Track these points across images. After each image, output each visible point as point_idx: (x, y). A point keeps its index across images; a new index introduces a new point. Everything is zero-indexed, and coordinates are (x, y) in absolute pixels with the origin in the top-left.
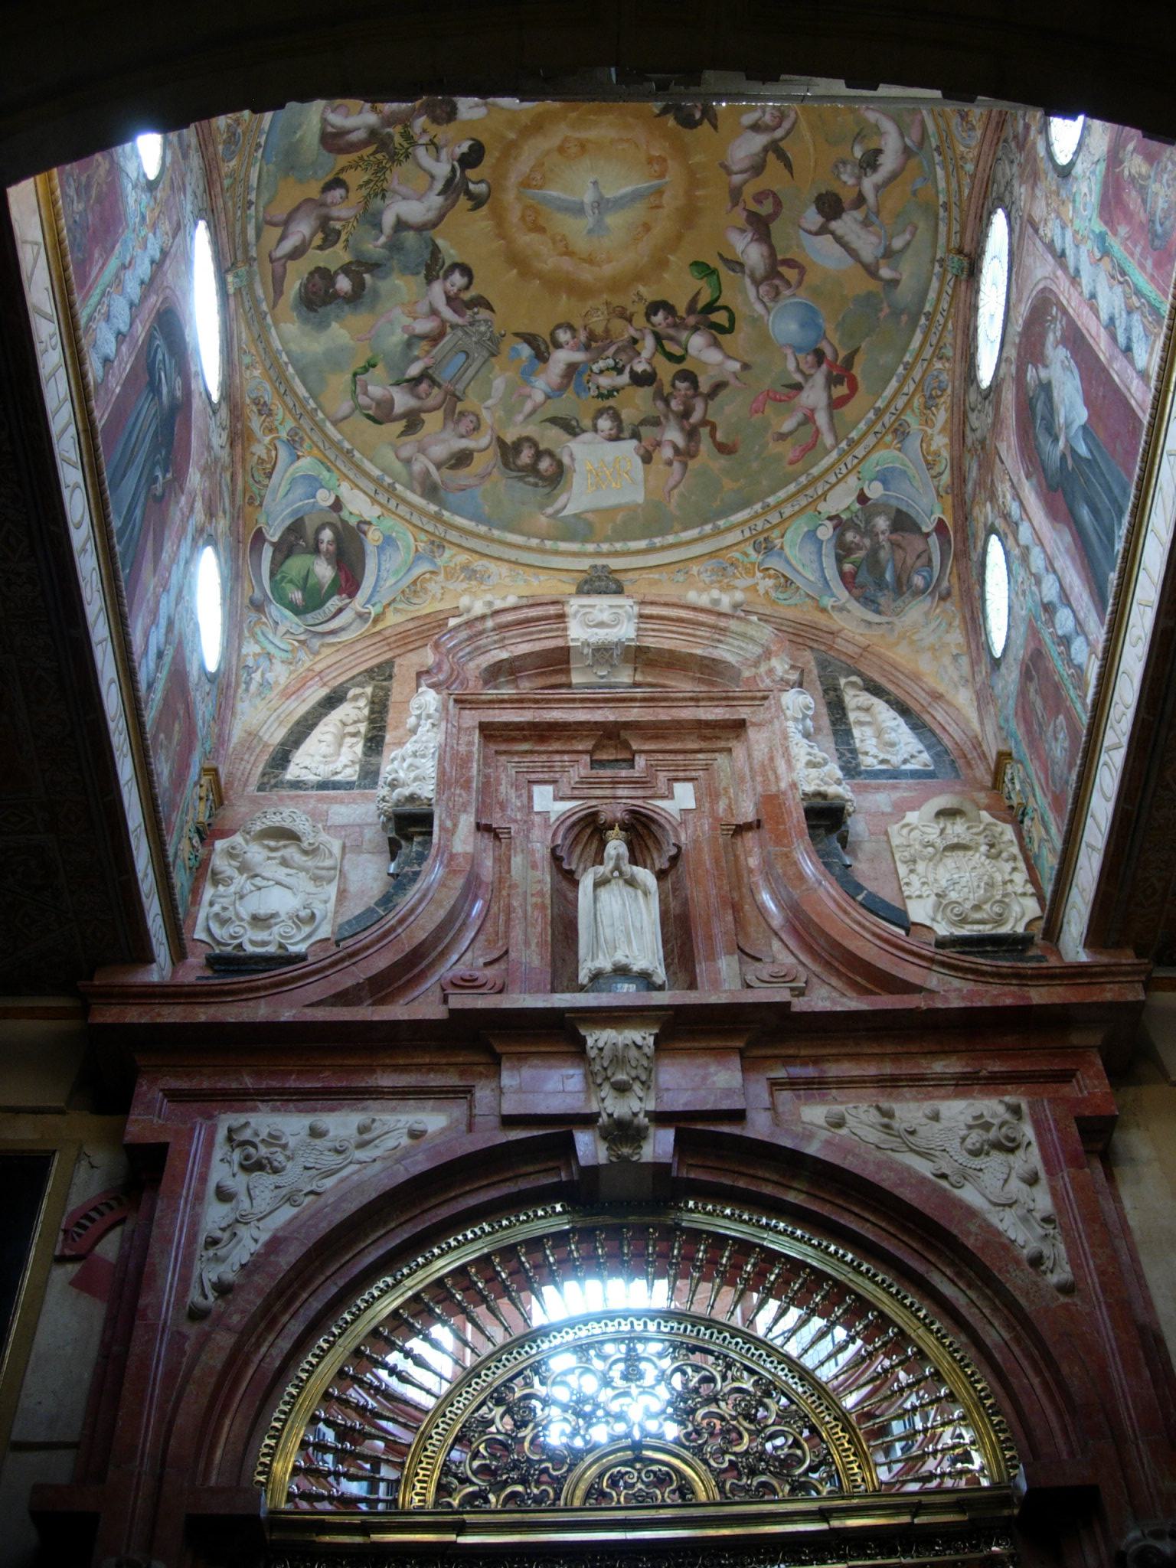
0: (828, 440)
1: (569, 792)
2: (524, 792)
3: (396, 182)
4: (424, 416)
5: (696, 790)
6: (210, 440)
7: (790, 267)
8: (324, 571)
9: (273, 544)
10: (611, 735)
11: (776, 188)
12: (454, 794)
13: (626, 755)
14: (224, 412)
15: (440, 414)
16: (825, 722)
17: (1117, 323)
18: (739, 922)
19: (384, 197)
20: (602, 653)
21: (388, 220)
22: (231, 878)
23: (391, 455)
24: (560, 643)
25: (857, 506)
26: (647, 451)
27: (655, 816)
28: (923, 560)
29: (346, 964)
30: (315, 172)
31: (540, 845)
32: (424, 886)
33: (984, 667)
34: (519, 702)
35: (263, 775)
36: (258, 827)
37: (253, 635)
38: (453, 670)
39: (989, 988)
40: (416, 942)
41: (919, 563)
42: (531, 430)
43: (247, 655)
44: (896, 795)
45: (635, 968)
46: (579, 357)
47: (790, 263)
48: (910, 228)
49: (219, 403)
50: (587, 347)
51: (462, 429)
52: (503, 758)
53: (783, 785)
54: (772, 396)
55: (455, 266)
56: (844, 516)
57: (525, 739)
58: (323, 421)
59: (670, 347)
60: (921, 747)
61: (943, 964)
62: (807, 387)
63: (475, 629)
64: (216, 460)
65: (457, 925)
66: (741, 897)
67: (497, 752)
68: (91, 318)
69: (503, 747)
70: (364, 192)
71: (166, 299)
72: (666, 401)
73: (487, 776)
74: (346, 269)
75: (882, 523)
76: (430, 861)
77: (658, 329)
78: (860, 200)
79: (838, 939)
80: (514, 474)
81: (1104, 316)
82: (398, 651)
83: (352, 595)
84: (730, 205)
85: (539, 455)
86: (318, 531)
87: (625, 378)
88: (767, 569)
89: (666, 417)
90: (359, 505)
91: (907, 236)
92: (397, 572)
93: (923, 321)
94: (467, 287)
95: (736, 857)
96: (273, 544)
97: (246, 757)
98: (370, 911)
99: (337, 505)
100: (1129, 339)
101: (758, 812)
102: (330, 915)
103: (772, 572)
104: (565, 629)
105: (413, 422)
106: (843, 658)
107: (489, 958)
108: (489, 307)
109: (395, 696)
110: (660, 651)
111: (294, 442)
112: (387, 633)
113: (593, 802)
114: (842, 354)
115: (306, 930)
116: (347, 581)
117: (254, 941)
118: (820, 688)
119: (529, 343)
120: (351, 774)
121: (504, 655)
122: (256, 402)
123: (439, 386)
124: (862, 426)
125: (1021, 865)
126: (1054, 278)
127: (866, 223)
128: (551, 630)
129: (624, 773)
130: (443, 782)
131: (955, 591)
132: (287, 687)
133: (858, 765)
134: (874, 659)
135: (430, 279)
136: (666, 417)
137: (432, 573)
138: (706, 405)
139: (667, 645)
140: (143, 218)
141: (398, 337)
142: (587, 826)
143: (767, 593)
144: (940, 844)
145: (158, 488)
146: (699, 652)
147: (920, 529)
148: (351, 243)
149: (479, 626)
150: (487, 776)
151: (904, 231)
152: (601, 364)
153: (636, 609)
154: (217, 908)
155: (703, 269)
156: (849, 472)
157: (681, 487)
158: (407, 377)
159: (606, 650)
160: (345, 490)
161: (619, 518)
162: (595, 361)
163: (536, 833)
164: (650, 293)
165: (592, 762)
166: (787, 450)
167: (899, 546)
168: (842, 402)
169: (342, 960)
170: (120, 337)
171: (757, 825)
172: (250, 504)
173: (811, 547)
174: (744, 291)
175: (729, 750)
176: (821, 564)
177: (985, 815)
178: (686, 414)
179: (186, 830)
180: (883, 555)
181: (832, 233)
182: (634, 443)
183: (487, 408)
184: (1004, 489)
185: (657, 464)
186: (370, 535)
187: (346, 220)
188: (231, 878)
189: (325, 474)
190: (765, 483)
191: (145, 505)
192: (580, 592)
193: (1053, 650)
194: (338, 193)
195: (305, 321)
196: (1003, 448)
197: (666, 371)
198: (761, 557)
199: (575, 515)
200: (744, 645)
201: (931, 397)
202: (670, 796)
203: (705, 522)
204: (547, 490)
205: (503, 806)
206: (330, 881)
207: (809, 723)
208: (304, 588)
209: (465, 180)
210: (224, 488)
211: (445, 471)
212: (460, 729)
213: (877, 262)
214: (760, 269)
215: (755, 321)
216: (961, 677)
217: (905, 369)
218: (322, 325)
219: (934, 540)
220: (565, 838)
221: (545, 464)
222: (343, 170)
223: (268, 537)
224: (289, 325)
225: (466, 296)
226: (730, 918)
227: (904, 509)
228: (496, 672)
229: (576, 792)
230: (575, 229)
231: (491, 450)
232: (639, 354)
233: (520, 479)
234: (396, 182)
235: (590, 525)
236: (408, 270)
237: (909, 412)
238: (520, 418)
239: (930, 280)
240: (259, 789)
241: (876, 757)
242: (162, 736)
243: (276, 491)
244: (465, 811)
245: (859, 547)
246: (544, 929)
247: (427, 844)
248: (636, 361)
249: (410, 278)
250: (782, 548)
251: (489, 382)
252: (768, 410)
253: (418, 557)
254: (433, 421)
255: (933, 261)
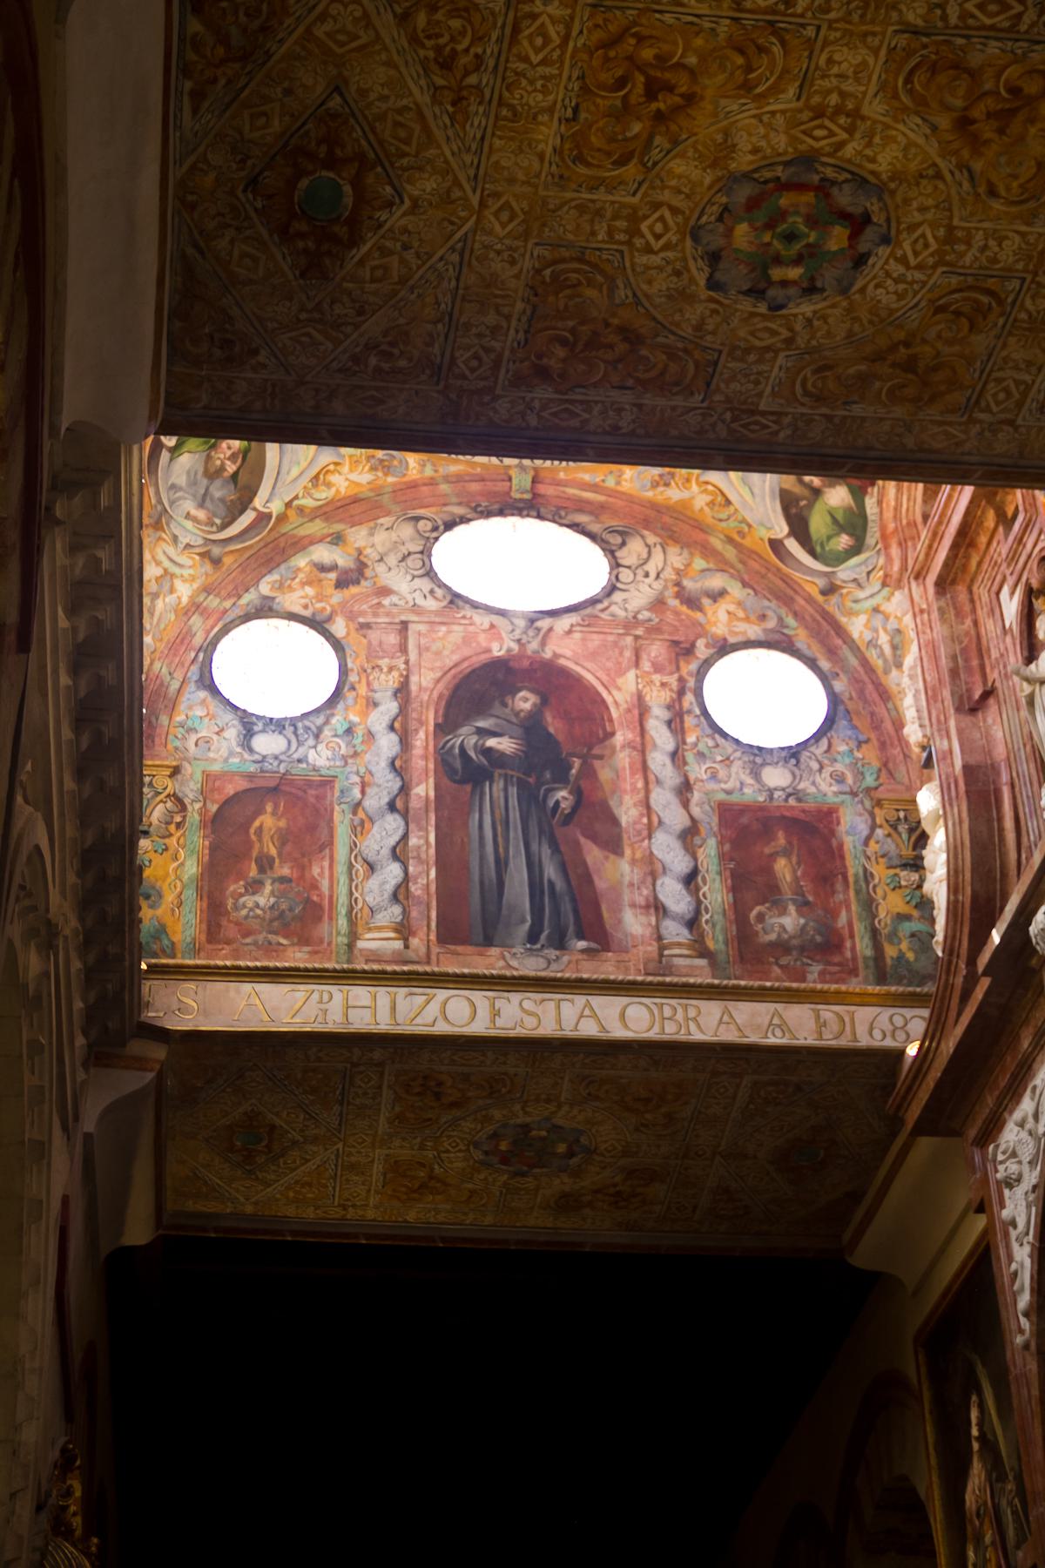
9: (789, 535)
37: (851, 613)
57: (967, 557)
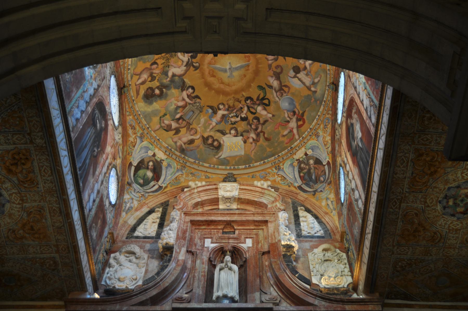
0: (297, 137)
1: (215, 241)
2: (202, 241)
3: (172, 63)
4: (180, 129)
5: (253, 241)
6: (114, 138)
7: (286, 87)
8: (150, 174)
9: (135, 166)
10: (229, 224)
11: (281, 64)
12: (181, 242)
13: (233, 230)
14: (120, 129)
15: (185, 129)
16: (293, 221)
17: (368, 109)
18: (261, 282)
19: (169, 67)
20: (227, 199)
21: (170, 74)
22: (114, 266)
23: (171, 141)
24: (216, 196)
25: (305, 157)
26: (245, 140)
27: (240, 249)
28: (323, 173)
29: (144, 293)
30: (148, 60)
31: (205, 257)
32: (169, 269)
33: (339, 205)
34: (202, 214)
35: (128, 234)
36: (124, 250)
37: (128, 193)
38: (184, 204)
39: (333, 305)
40: (165, 286)
41: (322, 174)
42: (212, 134)
43: (126, 198)
44: (311, 243)
45: (229, 295)
46: (226, 113)
47: (286, 86)
48: (319, 76)
49: (118, 126)
50: (228, 110)
51: (192, 133)
52: (197, 231)
53: (276, 240)
54: (281, 124)
55: (190, 87)
56: (301, 160)
57: (204, 225)
58: (151, 131)
59: (252, 110)
60: (321, 229)
61: (319, 297)
62: (291, 122)
63: (191, 192)
64: (117, 143)
65: (178, 281)
66: (263, 274)
67: (195, 229)
68: (72, 108)
69: (197, 227)
70: (163, 66)
71: (99, 99)
72: (251, 126)
73: (191, 236)
74: (158, 88)
75: (312, 162)
76: (171, 262)
77: (248, 105)
78: (305, 68)
79: (289, 288)
80: (207, 146)
81: (365, 107)
82: (170, 198)
83: (158, 181)
84: (268, 70)
85: (214, 141)
86: (148, 162)
87: (239, 119)
88: (279, 175)
89: (251, 130)
90: (160, 155)
91: (319, 79)
92: (171, 174)
93: (323, 103)
94: (193, 92)
95: (262, 262)
96: (135, 166)
97: (123, 229)
98: (153, 277)
99: (154, 155)
100: (370, 114)
101: (269, 248)
102: (142, 277)
103: (280, 175)
104: (218, 192)
105: (177, 131)
106: (300, 201)
107: (187, 291)
108: (199, 98)
109: (168, 212)
110: (245, 199)
111: (142, 137)
112: (168, 192)
113: (222, 244)
114: (301, 112)
115: (134, 282)
116: (156, 177)
117: (119, 285)
118: (292, 210)
119: (211, 109)
120: (154, 234)
121: (200, 200)
122: (131, 125)
123: (185, 121)
124: (306, 133)
125: (348, 266)
126: (354, 94)
127: (307, 75)
128: (214, 193)
129: (232, 236)
130: (178, 238)
131: (332, 182)
132: (137, 208)
133: (301, 234)
134: (309, 202)
135: (182, 90)
136: (251, 130)
137: (182, 175)
138: (262, 127)
139: (247, 197)
140: (91, 77)
141: (173, 107)
142: (220, 251)
143: (278, 182)
144: (323, 260)
145: (95, 153)
146: (256, 199)
147: (322, 163)
148: (159, 80)
149: (193, 191)
150: (191, 236)
151: (317, 77)
152: (232, 115)
153: (239, 187)
154: (109, 275)
155: (261, 88)
156: (302, 146)
157: (255, 151)
158: (176, 118)
159: (230, 199)
160: (157, 151)
161: (237, 159)
162: (230, 114)
163: (205, 253)
164: (245, 94)
165: (223, 232)
166: (285, 140)
167: (317, 169)
168: (301, 126)
169: (143, 292)
170: (82, 112)
171: (268, 252)
172: (128, 155)
173: (291, 169)
174: (273, 94)
175: (263, 229)
176: (294, 173)
177: (338, 251)
178: (256, 129)
179: (102, 251)
180: (312, 171)
181: (298, 77)
182: (241, 137)
183: (199, 127)
184: (343, 154)
185: (247, 144)
186: (164, 164)
187: (158, 74)
188: (114, 266)
189: (151, 146)
190: (279, 149)
191: (90, 159)
192: (224, 181)
193: (354, 203)
194: (155, 66)
195: (146, 102)
196: (343, 141)
197: (251, 117)
198: (277, 171)
199: (224, 158)
200: (269, 198)
201: (326, 125)
202: (245, 242)
203: (262, 161)
204: (216, 151)
205: (195, 245)
206: (143, 267)
207: (287, 221)
208: (143, 179)
209: (192, 62)
210: (120, 150)
211: (186, 145)
212: (184, 222)
213: (310, 86)
214: (277, 88)
215: (276, 102)
216: (333, 208)
217: (318, 117)
218: (151, 103)
219: (326, 167)
220: (212, 255)
221: (216, 143)
222: (156, 59)
223: (133, 164)
224: (141, 104)
225: (193, 95)
226: (258, 280)
227: (318, 157)
228: (196, 205)
229: (218, 241)
230: (225, 76)
231: (200, 139)
232: (243, 112)
233: (208, 147)
234: (172, 63)
235: (228, 161)
236: (176, 88)
237: (319, 129)
238: (208, 130)
239: (325, 91)
240: (126, 238)
241: (307, 232)
242: (94, 225)
243: (136, 151)
244: (184, 247)
245: (305, 169)
246: (204, 283)
247: (171, 256)
248: (242, 114)
249: (177, 90)
250: (283, 168)
251: (200, 120)
252: (280, 128)
253: (178, 170)
254: (183, 131)
255: (326, 86)
